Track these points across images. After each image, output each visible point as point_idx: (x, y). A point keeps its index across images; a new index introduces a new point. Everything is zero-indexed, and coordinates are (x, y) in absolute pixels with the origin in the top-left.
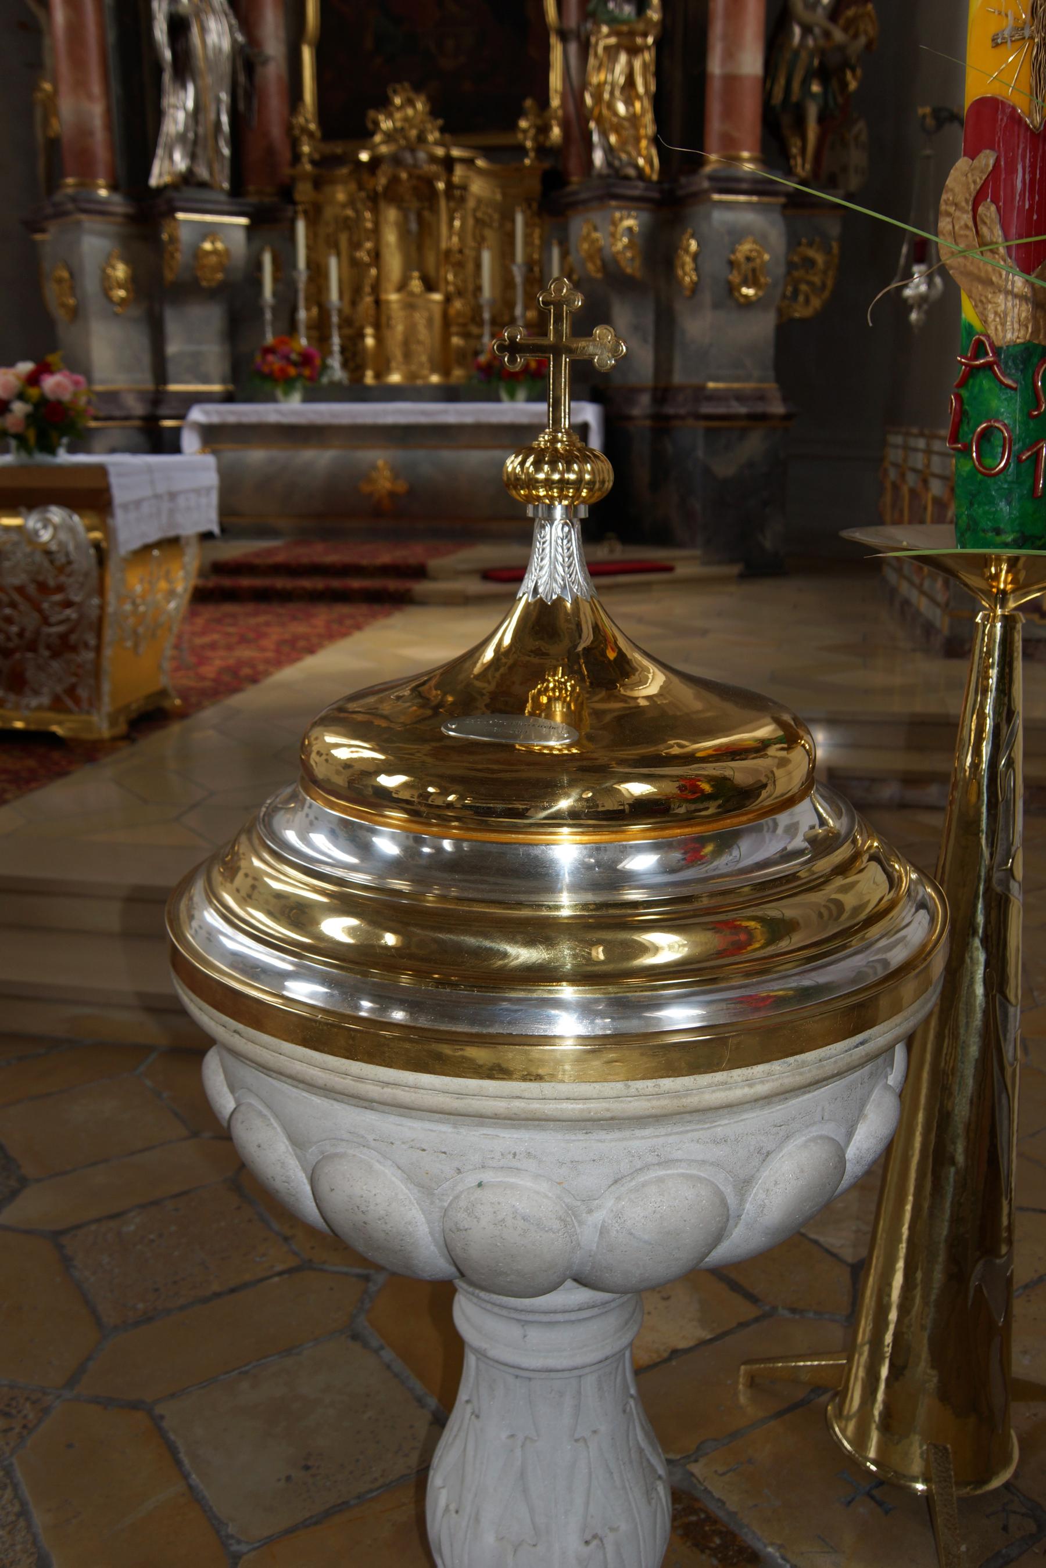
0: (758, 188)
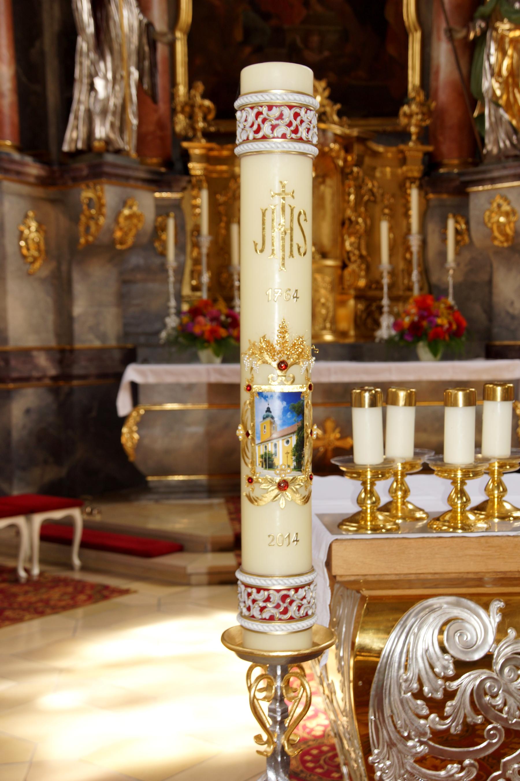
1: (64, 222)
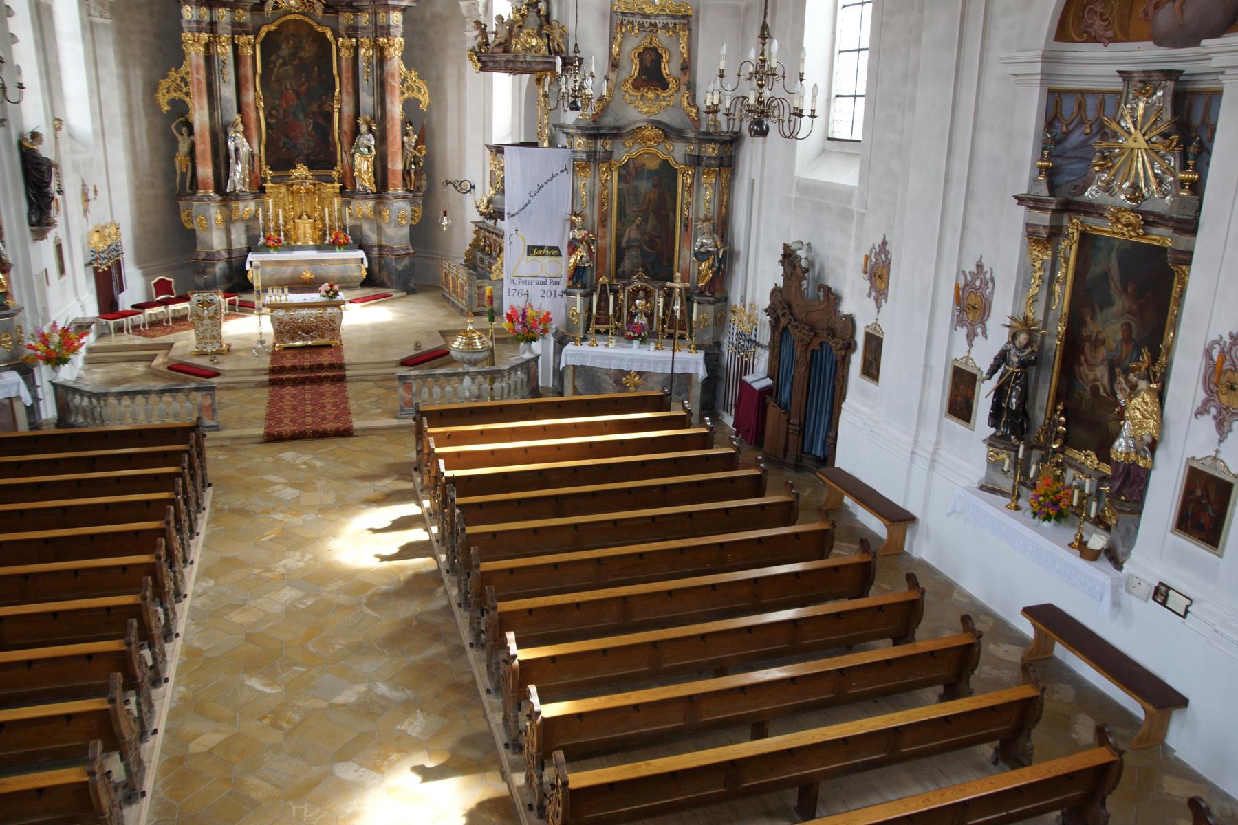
0: (404, 197)
1: (228, 212)
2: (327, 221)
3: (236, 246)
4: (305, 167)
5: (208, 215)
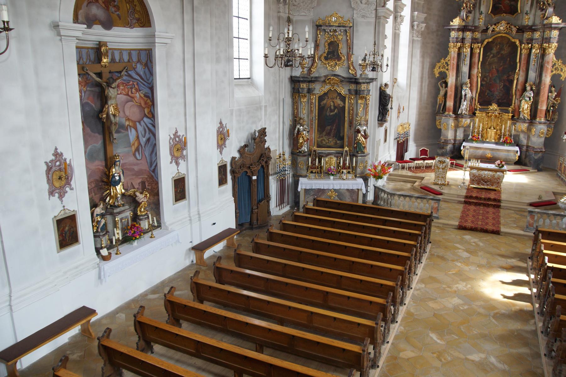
0: (544, 123)
1: (457, 122)
2: (503, 131)
3: (458, 138)
4: (496, 105)
5: (448, 124)
